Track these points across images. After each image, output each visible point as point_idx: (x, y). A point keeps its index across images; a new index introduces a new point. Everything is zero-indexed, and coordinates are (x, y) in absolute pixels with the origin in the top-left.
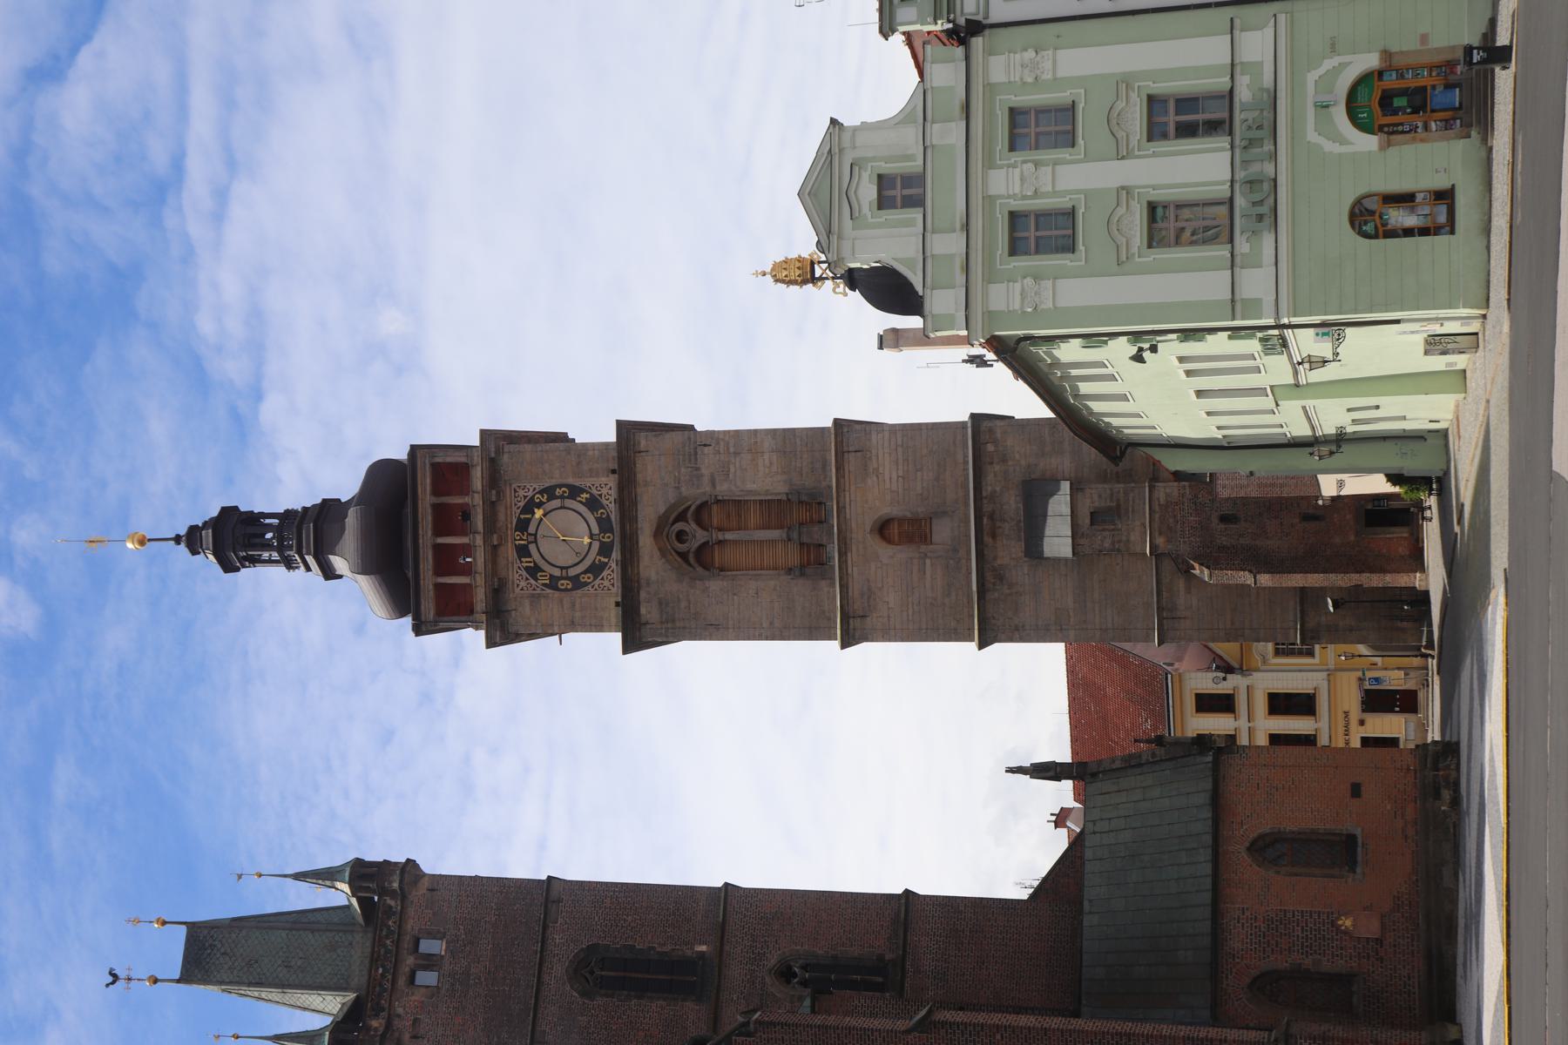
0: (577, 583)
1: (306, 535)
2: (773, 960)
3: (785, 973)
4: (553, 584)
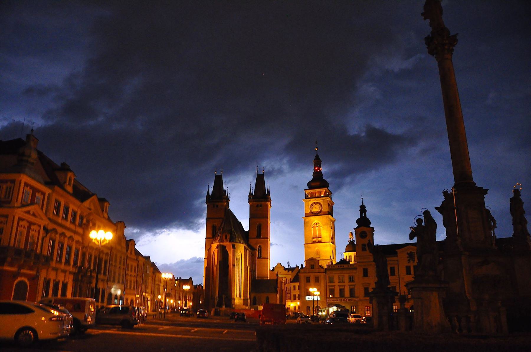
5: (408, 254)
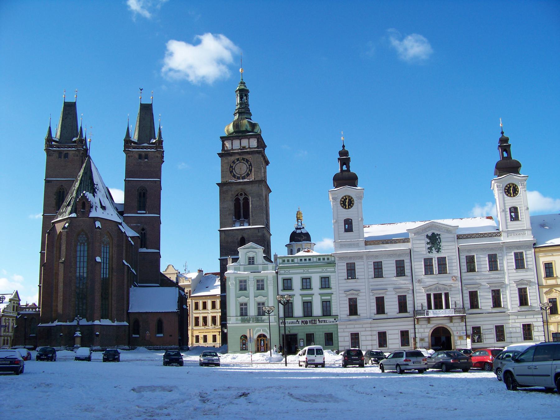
0: (231, 172)
1: (244, 110)
2: (145, 227)
3: (143, 229)
4: (231, 167)
5: (427, 236)
